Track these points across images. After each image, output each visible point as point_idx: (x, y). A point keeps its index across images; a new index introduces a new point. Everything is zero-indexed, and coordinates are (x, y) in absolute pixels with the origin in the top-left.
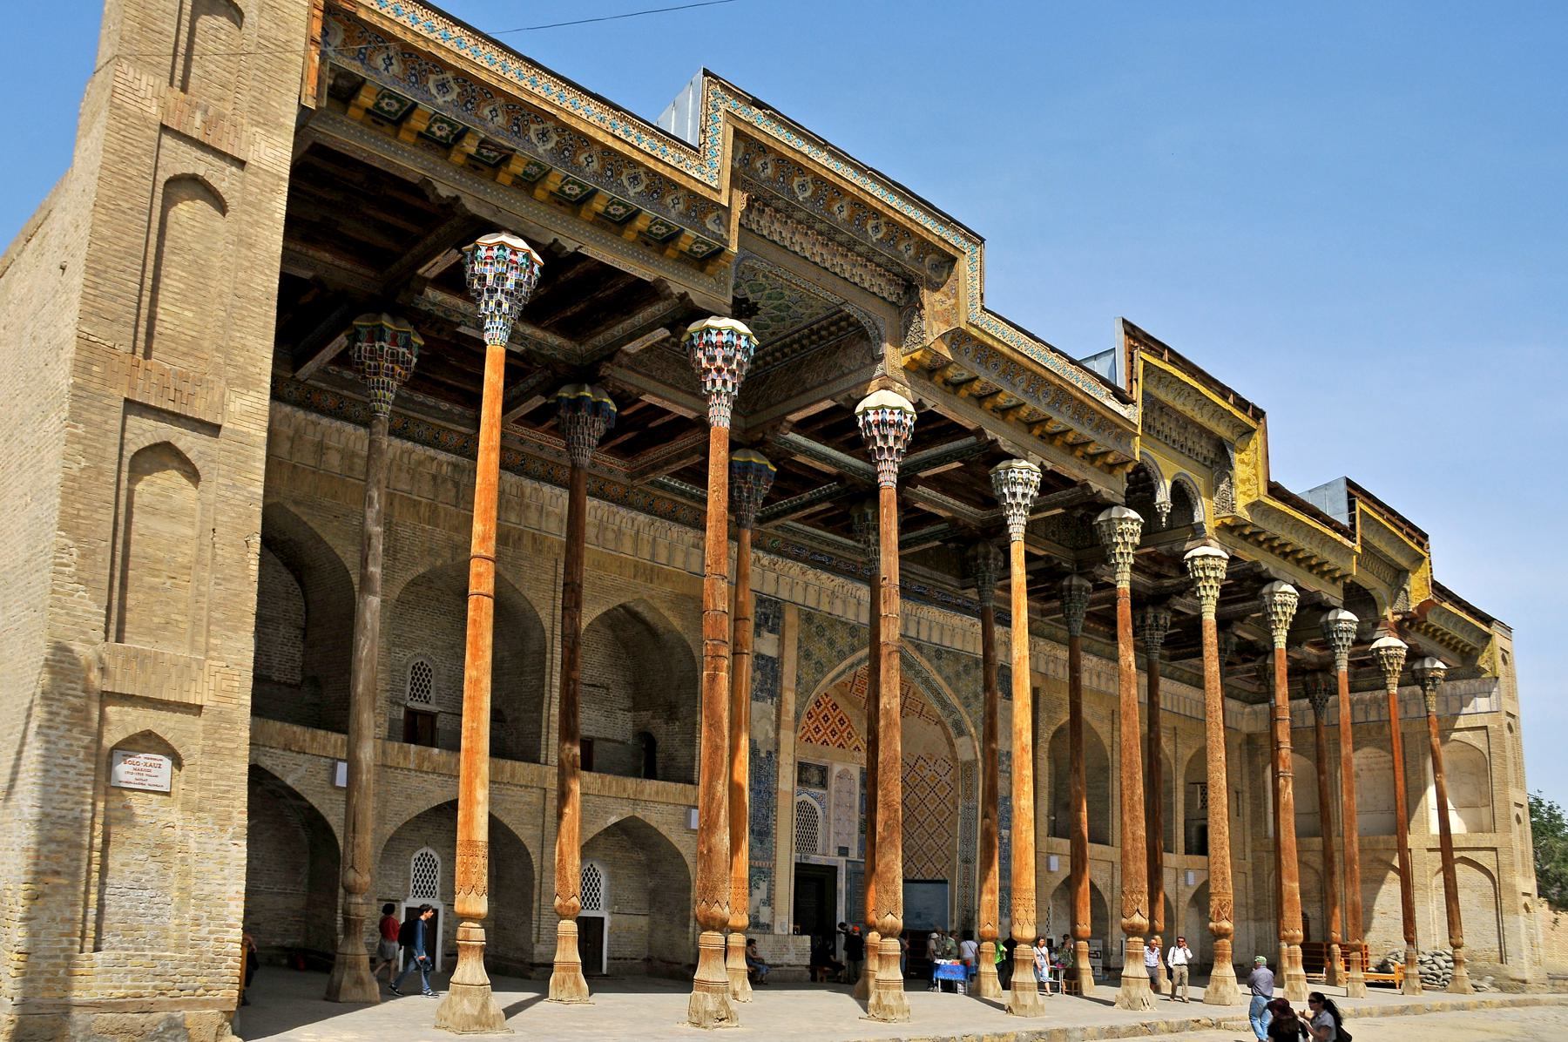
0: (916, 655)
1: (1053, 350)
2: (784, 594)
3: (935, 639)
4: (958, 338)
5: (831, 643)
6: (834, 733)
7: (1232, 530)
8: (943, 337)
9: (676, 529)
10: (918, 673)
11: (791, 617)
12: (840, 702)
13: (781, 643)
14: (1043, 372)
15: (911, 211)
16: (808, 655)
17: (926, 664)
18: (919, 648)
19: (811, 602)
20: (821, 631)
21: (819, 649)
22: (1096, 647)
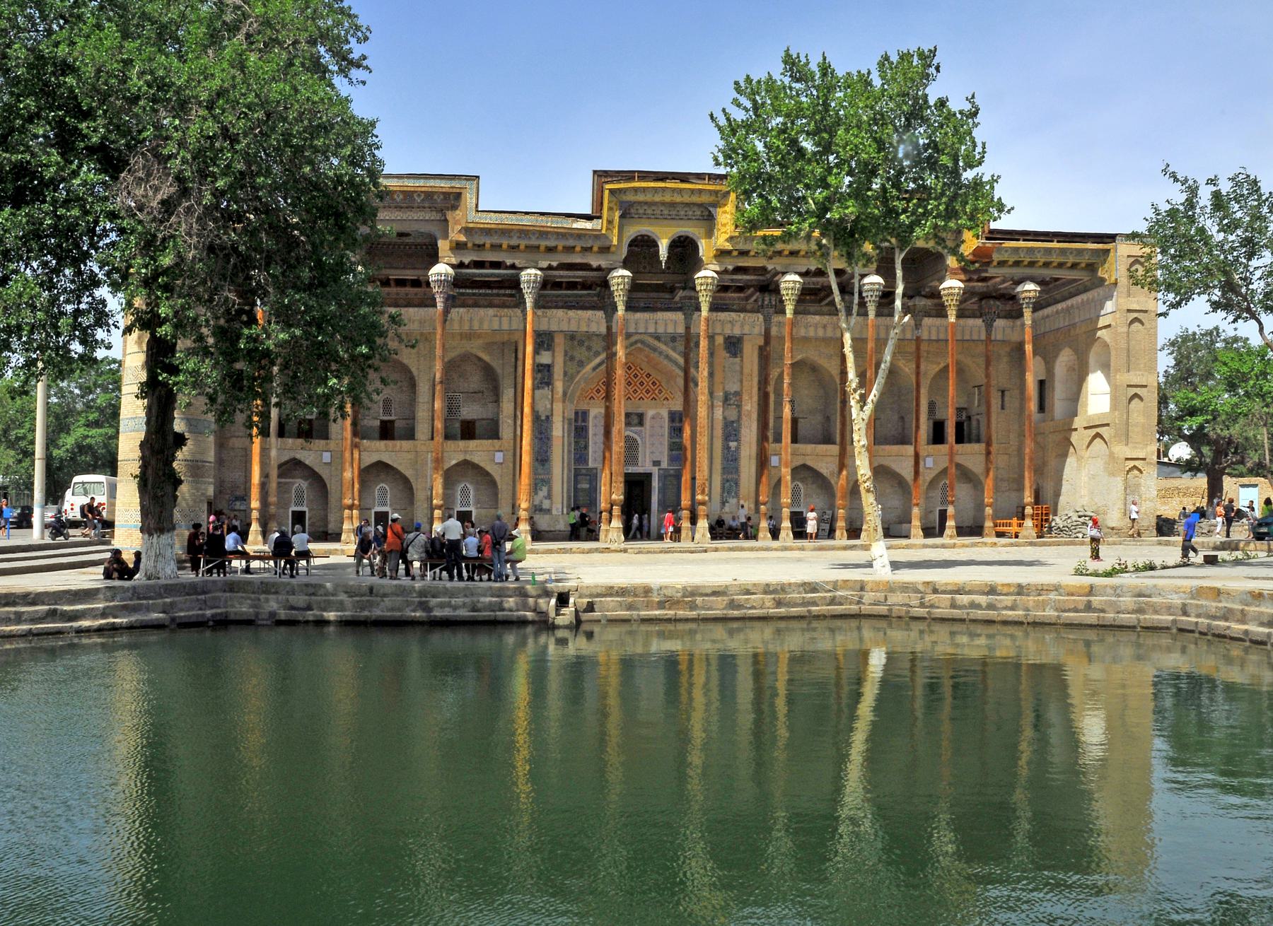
0: (656, 343)
1: (527, 213)
2: (554, 328)
3: (670, 330)
4: (467, 231)
5: (589, 348)
6: (648, 391)
7: (722, 254)
8: (460, 231)
9: (482, 311)
10: (661, 353)
11: (559, 341)
12: (653, 374)
13: (553, 356)
14: (543, 221)
15: (431, 183)
16: (572, 358)
17: (663, 347)
18: (658, 338)
19: (573, 327)
20: (581, 343)
21: (580, 353)
22: (812, 309)
